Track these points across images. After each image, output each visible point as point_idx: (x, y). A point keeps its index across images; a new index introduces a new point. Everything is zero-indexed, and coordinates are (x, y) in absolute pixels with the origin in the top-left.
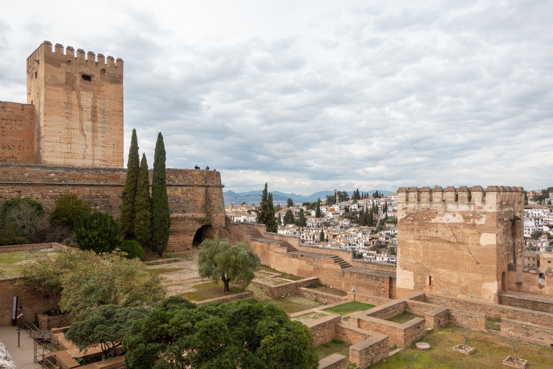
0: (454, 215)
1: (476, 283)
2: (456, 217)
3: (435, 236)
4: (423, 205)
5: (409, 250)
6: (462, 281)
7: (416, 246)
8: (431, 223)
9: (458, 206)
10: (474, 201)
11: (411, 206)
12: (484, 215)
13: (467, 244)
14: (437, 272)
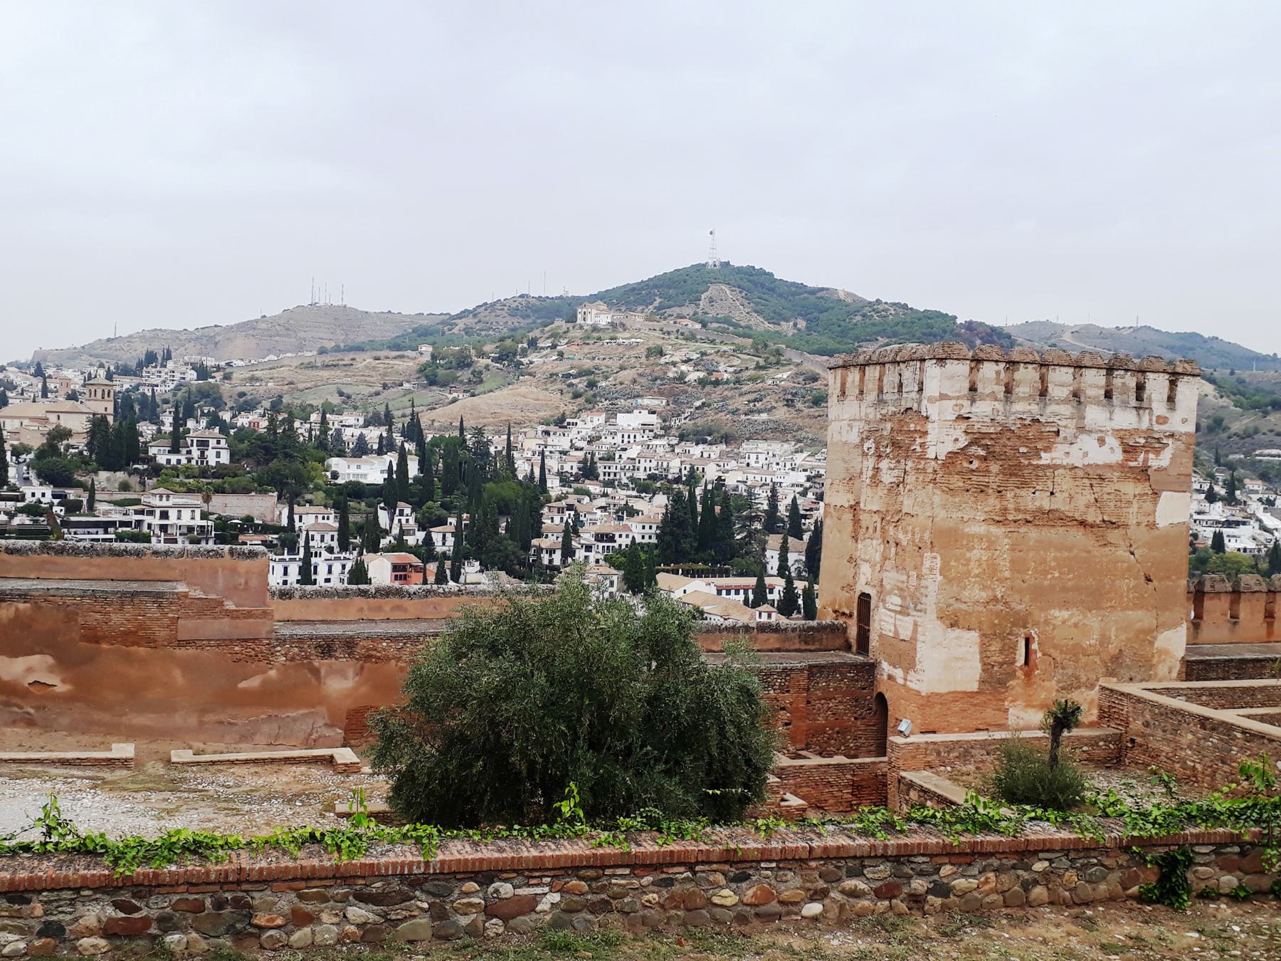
0: (1102, 441)
1: (1141, 636)
2: (1106, 447)
3: (1047, 508)
4: (1019, 407)
5: (969, 560)
6: (1110, 638)
7: (991, 544)
8: (1038, 466)
9: (1111, 413)
10: (1150, 400)
11: (983, 410)
12: (1170, 441)
13: (1126, 526)
14: (1047, 622)
